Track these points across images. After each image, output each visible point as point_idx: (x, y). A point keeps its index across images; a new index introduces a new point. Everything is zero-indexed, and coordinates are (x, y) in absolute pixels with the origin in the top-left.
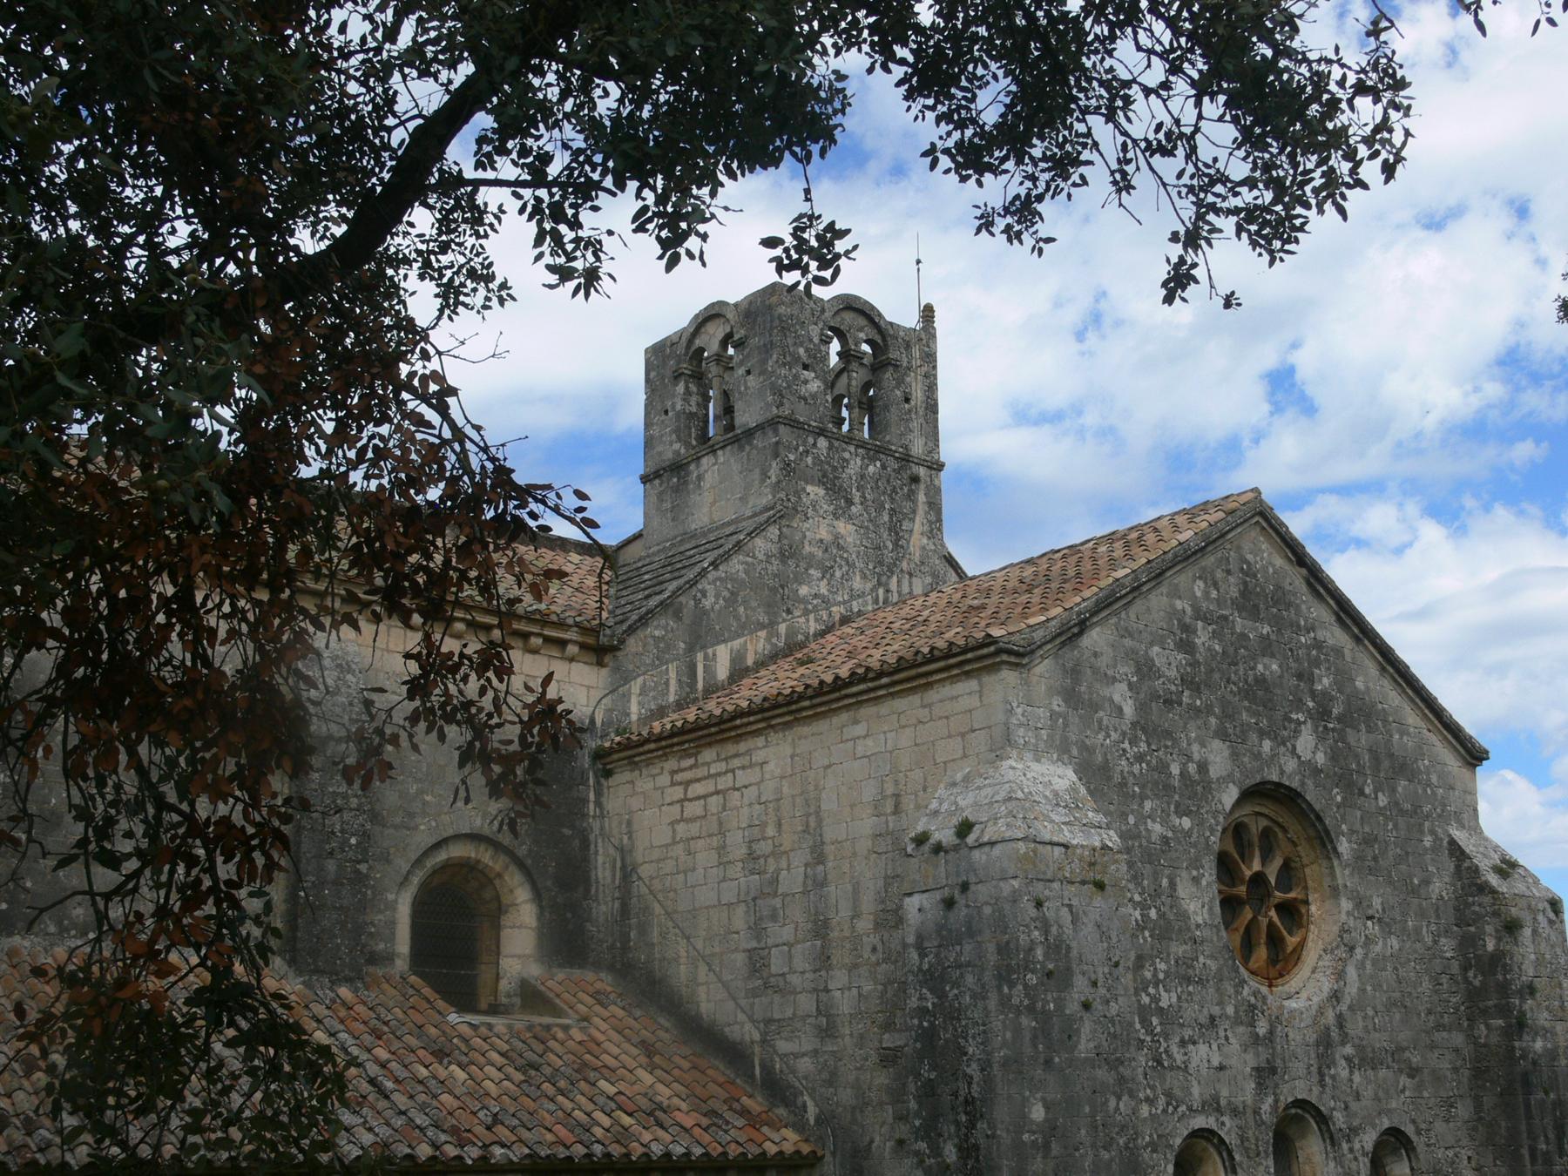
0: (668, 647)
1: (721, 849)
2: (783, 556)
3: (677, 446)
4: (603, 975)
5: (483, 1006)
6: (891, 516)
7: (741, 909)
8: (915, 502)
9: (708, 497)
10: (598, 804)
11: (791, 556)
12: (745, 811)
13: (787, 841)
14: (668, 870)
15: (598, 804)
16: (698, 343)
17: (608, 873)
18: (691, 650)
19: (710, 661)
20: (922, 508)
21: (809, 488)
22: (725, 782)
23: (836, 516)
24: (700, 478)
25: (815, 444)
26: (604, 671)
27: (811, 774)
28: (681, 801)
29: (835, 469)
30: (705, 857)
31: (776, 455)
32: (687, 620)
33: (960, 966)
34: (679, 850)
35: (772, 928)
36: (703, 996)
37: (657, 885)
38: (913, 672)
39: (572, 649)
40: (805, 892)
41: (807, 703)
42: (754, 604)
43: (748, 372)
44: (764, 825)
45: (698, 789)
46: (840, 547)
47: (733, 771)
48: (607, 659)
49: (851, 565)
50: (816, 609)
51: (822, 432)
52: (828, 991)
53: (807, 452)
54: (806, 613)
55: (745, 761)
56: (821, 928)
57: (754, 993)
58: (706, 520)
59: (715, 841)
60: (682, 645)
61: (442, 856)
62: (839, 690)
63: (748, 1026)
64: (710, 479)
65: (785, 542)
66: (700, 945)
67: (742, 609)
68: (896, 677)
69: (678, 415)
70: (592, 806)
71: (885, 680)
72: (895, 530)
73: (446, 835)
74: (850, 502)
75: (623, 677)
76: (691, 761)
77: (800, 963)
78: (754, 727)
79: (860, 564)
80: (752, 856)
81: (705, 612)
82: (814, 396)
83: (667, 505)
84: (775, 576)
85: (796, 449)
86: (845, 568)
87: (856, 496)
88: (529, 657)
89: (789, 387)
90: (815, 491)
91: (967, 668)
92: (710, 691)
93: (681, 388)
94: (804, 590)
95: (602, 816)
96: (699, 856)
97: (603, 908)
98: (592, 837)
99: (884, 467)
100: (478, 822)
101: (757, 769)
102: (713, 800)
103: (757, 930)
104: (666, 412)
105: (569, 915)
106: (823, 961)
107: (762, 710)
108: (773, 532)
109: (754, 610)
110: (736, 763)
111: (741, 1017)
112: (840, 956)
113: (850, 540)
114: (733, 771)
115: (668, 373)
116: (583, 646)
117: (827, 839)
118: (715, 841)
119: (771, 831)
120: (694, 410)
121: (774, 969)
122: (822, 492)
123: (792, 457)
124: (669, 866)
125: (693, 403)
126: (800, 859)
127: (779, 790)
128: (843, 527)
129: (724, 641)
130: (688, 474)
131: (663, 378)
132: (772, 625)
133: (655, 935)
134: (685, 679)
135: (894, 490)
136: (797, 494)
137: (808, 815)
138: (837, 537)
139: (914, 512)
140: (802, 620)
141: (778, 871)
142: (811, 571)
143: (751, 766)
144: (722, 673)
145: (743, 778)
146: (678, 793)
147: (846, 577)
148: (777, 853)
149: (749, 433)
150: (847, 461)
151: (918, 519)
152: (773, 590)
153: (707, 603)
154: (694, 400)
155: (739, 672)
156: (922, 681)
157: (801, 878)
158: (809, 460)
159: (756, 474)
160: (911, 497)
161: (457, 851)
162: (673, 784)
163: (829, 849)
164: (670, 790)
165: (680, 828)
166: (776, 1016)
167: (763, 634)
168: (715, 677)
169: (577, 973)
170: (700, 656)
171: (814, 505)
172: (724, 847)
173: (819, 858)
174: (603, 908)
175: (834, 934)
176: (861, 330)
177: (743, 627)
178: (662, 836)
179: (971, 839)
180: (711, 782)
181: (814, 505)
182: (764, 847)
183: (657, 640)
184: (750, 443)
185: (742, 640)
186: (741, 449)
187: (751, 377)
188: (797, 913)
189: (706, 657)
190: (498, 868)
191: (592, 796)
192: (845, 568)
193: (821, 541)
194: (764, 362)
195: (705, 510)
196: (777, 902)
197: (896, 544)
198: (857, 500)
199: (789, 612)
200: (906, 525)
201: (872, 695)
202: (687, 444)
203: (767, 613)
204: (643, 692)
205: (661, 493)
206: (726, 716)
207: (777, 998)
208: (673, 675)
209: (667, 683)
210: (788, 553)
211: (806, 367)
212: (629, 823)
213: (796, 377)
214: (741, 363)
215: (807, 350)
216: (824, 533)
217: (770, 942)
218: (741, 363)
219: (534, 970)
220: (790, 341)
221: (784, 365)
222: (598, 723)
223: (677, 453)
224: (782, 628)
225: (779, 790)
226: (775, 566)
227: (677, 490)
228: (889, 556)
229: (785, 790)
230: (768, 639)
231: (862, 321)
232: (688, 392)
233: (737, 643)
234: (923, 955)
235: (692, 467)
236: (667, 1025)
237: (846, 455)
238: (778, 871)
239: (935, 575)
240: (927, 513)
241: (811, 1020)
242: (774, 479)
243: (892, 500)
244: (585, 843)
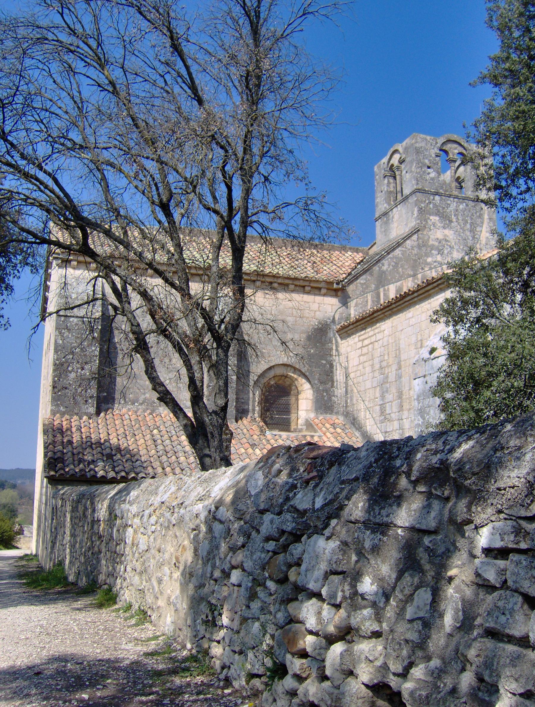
0: (367, 287)
1: (372, 365)
2: (419, 247)
3: (385, 205)
4: (339, 417)
5: (292, 430)
6: (471, 226)
7: (378, 389)
8: (483, 219)
9: (395, 225)
10: (337, 350)
11: (424, 246)
12: (379, 350)
13: (391, 361)
14: (358, 375)
15: (337, 350)
16: (391, 162)
17: (341, 377)
18: (377, 288)
21: (431, 218)
22: (373, 339)
23: (444, 228)
24: (393, 217)
25: (434, 199)
27: (397, 333)
28: (361, 348)
29: (444, 208)
30: (368, 369)
31: (416, 205)
32: (375, 276)
33: (429, 407)
34: (361, 367)
35: (387, 395)
36: (368, 424)
37: (355, 382)
38: (423, 291)
39: (323, 291)
40: (396, 381)
41: (394, 306)
42: (406, 267)
44: (384, 355)
45: (366, 342)
46: (446, 241)
48: (339, 293)
49: (452, 248)
50: (435, 267)
51: (437, 194)
52: (402, 419)
53: (430, 202)
54: (431, 269)
56: (400, 395)
57: (382, 422)
58: (395, 234)
59: (370, 363)
60: (374, 286)
61: (272, 374)
62: (403, 299)
63: (380, 435)
64: (396, 217)
65: (421, 241)
66: (367, 404)
67: (400, 270)
68: (420, 292)
69: (385, 193)
70: (334, 351)
71: (416, 295)
72: (473, 231)
73: (272, 364)
74: (451, 221)
75: (345, 301)
76: (364, 332)
77: (395, 409)
78: (380, 317)
80: (381, 368)
81: (384, 272)
82: (432, 179)
83: (383, 230)
84: (416, 255)
85: (425, 202)
86: (449, 249)
87: (454, 219)
89: (421, 176)
91: (440, 287)
93: (386, 181)
94: (429, 260)
95: (339, 355)
96: (367, 369)
97: (340, 391)
98: (334, 364)
99: (467, 205)
100: (286, 359)
102: (370, 346)
103: (383, 397)
105: (325, 394)
106: (401, 406)
108: (415, 237)
109: (406, 269)
110: (376, 331)
111: (378, 431)
112: (406, 406)
113: (451, 237)
115: (382, 176)
116: (328, 289)
117: (402, 360)
118: (370, 363)
119: (386, 357)
120: (392, 189)
121: (387, 412)
122: (437, 218)
123: (423, 205)
124: (358, 373)
126: (394, 367)
127: (388, 341)
129: (393, 283)
130: (389, 216)
132: (414, 276)
133: (355, 401)
134: (375, 299)
135: (472, 215)
136: (426, 220)
137: (396, 350)
139: (482, 223)
140: (429, 272)
141: (388, 373)
142: (433, 252)
143: (380, 332)
145: (379, 336)
146: (360, 344)
147: (450, 253)
148: (388, 366)
149: (407, 197)
150: (449, 204)
151: (485, 226)
152: (415, 261)
153: (385, 268)
154: (392, 185)
156: (427, 294)
157: (394, 376)
158: (431, 206)
159: (410, 214)
160: (481, 216)
161: (279, 371)
162: (359, 341)
163: (403, 363)
164: (358, 344)
165: (361, 358)
166: (388, 430)
167: (411, 279)
169: (328, 416)
170: (381, 290)
171: (434, 224)
172: (373, 365)
173: (400, 368)
174: (339, 391)
175: (404, 397)
176: (456, 149)
177: (401, 277)
178: (356, 362)
179: (432, 356)
180: (369, 339)
181: (434, 224)
182: (384, 364)
183: (362, 284)
185: (401, 282)
186: (405, 204)
188: (393, 390)
189: (384, 290)
190: (295, 376)
191: (334, 348)
193: (438, 239)
194: (411, 167)
195: (395, 230)
196: (388, 385)
197: (474, 237)
198: (454, 220)
199: (422, 269)
200: (478, 229)
201: (413, 300)
202: (389, 204)
203: (412, 270)
204: (356, 305)
205: (381, 225)
207: (388, 423)
208: (369, 298)
209: (367, 301)
210: (423, 244)
211: (429, 167)
212: (347, 357)
213: (424, 172)
214: (405, 168)
215: (429, 160)
217: (386, 401)
219: (312, 415)
220: (421, 158)
221: (419, 167)
222: (336, 318)
223: (385, 208)
224: (420, 276)
225: (388, 341)
226: (415, 251)
229: (390, 341)
230: (413, 281)
231: (455, 146)
232: (389, 183)
233: (398, 284)
234: (419, 403)
235: (390, 213)
236: (358, 435)
237: (449, 202)
238: (388, 373)
240: (489, 223)
241: (397, 431)
242: (416, 215)
243: (472, 219)
244: (332, 366)
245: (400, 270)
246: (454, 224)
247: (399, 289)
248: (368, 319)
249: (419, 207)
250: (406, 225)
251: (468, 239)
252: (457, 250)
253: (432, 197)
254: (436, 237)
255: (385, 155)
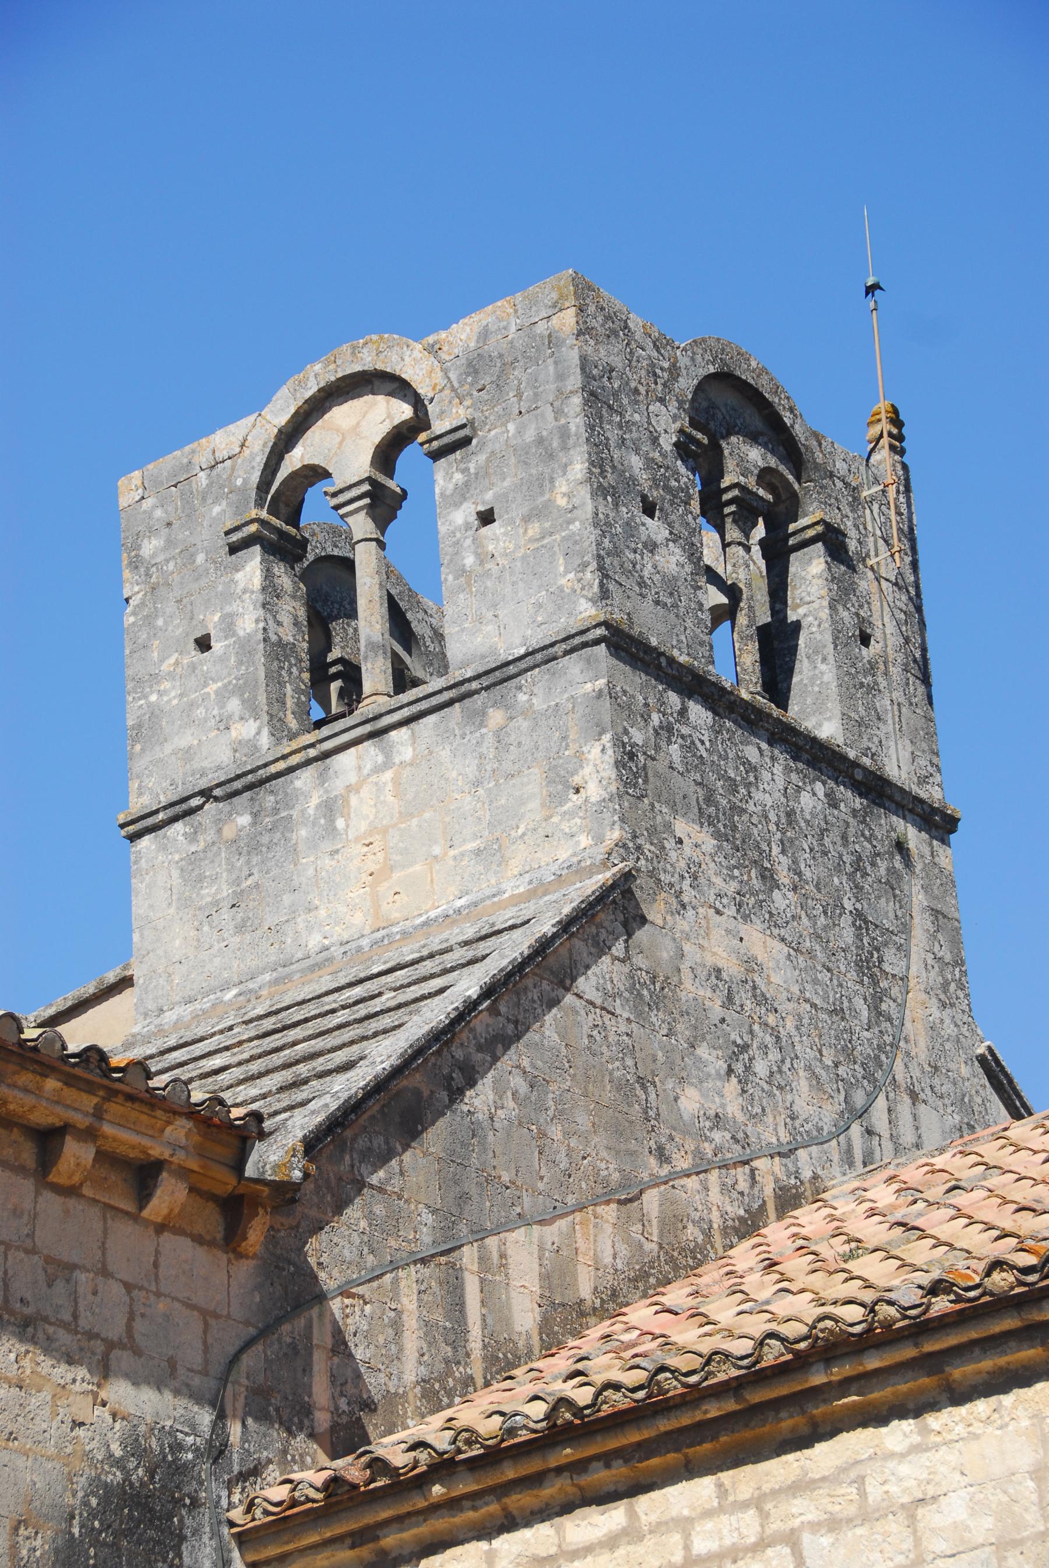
11: (656, 1003)
16: (296, 458)
19: (494, 1269)
20: (921, 924)
21: (681, 827)
24: (330, 808)
26: (244, 1269)
39: (169, 1196)
43: (487, 518)
46: (761, 999)
47: (792, 1539)
55: (843, 1500)
60: (428, 1218)
64: (363, 811)
69: (244, 648)
72: (868, 966)
79: (805, 1050)
85: (646, 719)
86: (774, 1055)
88: (51, 1203)
90: (694, 837)
92: (502, 1364)
99: (833, 802)
101: (895, 1526)
104: (204, 644)
107: (922, 1327)
110: (803, 1509)
113: (776, 979)
114: (792, 1539)
123: (638, 736)
125: (286, 619)
128: (757, 940)
131: (188, 553)
134: (438, 1316)
138: (751, 964)
139: (906, 929)
140: (692, 1183)
142: (702, 1051)
143: (866, 1516)
144: (525, 1318)
147: (778, 1082)
149: (500, 676)
155: (562, 1319)
159: (533, 783)
167: (610, 1212)
168: (506, 1321)
170: (468, 1256)
184: (501, 703)
186: (478, 718)
187: (495, 528)
189: (483, 1259)
192: (774, 1055)
194: (543, 483)
198: (784, 877)
199: (662, 1156)
200: (892, 962)
205: (193, 859)
206: (774, 1354)
208: (409, 1303)
209: (397, 1326)
210: (652, 993)
211: (649, 509)
213: (631, 529)
214: (462, 494)
215: (650, 463)
216: (719, 951)
218: (462, 494)
223: (253, 746)
227: (251, 846)
228: (865, 1041)
230: (621, 1226)
233: (552, 1233)
235: (304, 779)
239: (962, 1103)
242: (594, 792)
245: (556, 1132)
246: (782, 900)
247: (555, 1275)
248: (713, 1410)
249: (618, 743)
250: (491, 854)
251: (856, 1014)
252: (808, 1068)
253: (674, 699)
254: (710, 961)
255: (258, 404)
